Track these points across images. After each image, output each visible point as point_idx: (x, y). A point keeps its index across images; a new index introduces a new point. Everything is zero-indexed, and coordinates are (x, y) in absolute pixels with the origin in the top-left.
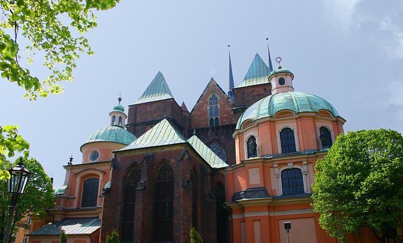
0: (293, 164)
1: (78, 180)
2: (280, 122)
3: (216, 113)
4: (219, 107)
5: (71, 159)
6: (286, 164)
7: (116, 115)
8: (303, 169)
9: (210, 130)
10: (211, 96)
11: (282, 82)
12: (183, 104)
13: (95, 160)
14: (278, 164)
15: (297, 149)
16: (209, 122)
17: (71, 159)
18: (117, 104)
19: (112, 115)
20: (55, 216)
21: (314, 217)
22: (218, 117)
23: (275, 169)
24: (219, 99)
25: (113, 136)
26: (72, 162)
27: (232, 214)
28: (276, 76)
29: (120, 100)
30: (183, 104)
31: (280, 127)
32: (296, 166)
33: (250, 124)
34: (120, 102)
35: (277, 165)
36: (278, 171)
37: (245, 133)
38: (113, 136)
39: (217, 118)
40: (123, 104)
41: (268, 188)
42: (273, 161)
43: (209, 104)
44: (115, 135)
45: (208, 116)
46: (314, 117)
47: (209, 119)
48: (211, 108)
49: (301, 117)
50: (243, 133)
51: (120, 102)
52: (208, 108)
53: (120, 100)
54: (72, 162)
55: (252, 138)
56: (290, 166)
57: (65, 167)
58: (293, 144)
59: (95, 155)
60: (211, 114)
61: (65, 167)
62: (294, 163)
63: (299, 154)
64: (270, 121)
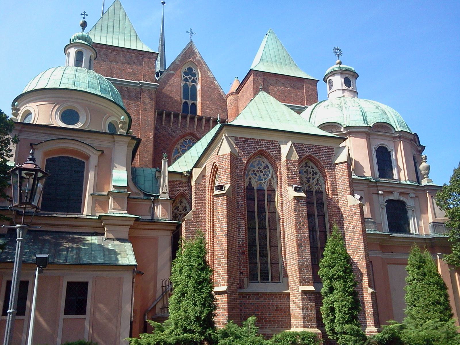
2: (376, 137)
11: (347, 82)
14: (384, 192)
29: (84, 25)
36: (383, 201)
62: (401, 194)
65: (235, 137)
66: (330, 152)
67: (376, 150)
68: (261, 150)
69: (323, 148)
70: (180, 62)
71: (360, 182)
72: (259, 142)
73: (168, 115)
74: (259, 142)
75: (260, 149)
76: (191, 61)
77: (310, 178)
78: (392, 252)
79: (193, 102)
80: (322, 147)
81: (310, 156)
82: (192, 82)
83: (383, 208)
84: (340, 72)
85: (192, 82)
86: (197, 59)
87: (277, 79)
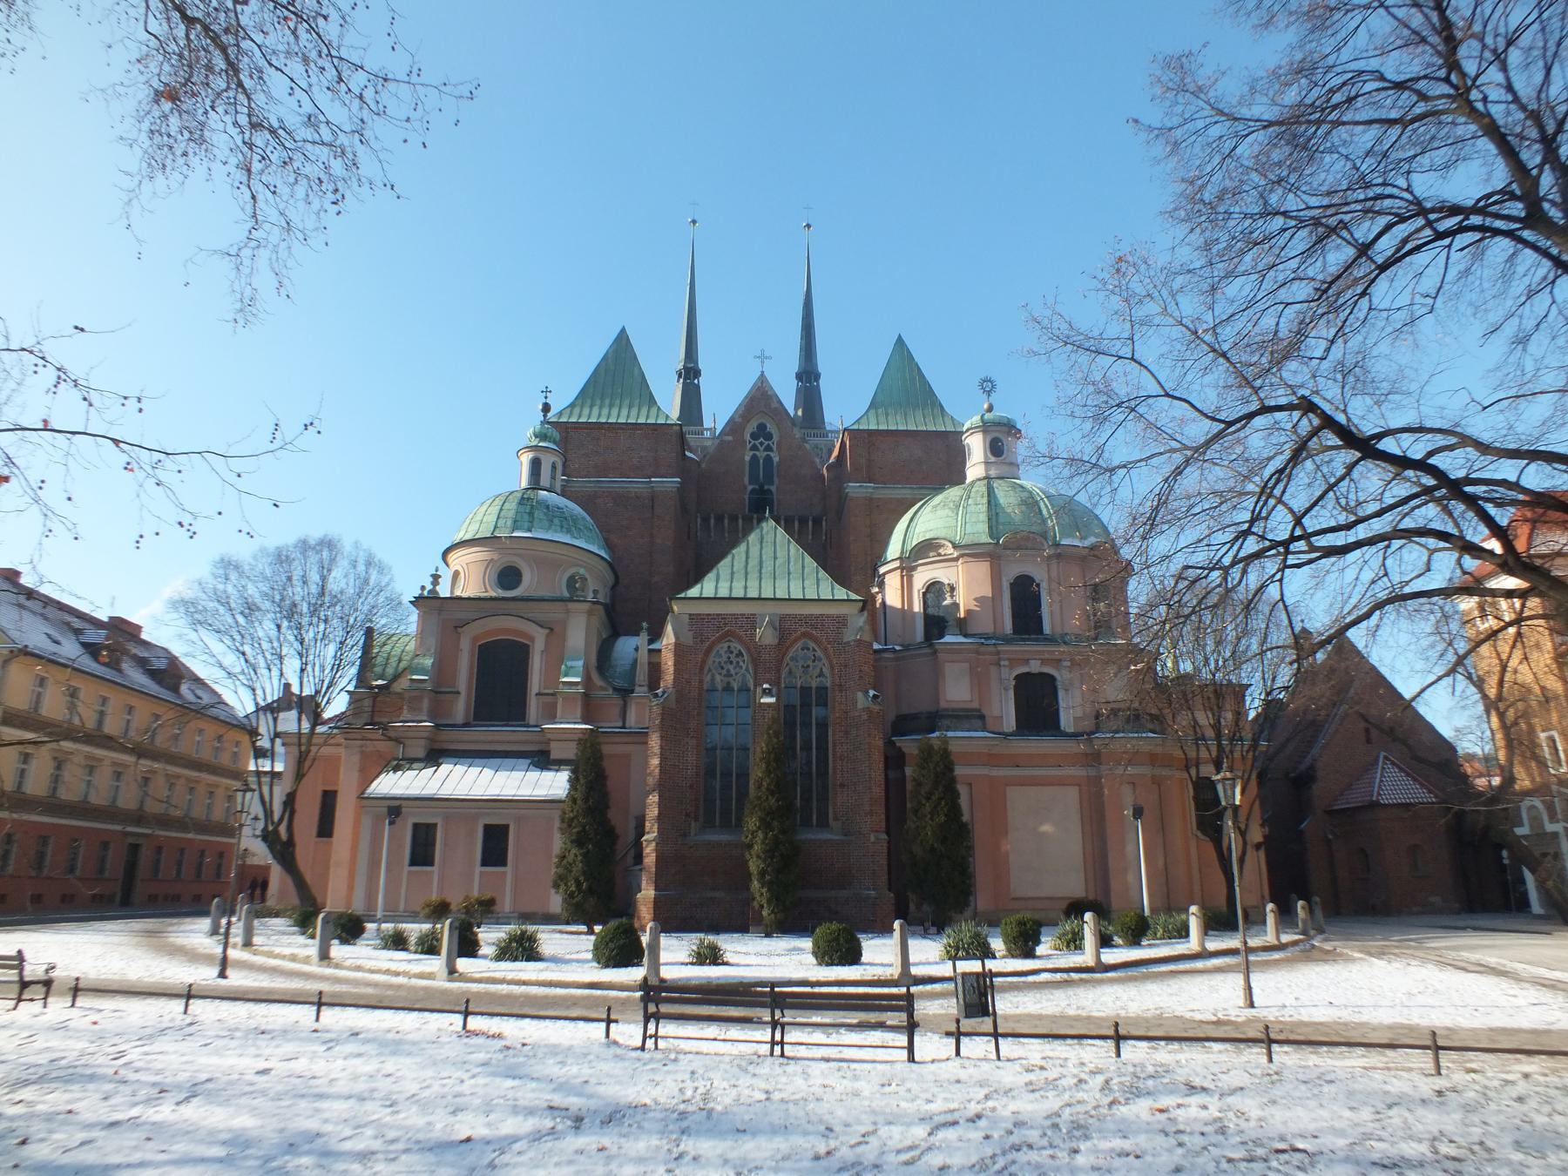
4: (776, 459)
6: (1027, 661)
8: (1062, 676)
15: (1047, 629)
20: (408, 742)
24: (775, 438)
32: (1047, 670)
36: (1010, 675)
43: (749, 446)
45: (746, 480)
46: (1083, 559)
48: (754, 458)
52: (747, 458)
56: (1035, 667)
59: (508, 576)
63: (1051, 640)
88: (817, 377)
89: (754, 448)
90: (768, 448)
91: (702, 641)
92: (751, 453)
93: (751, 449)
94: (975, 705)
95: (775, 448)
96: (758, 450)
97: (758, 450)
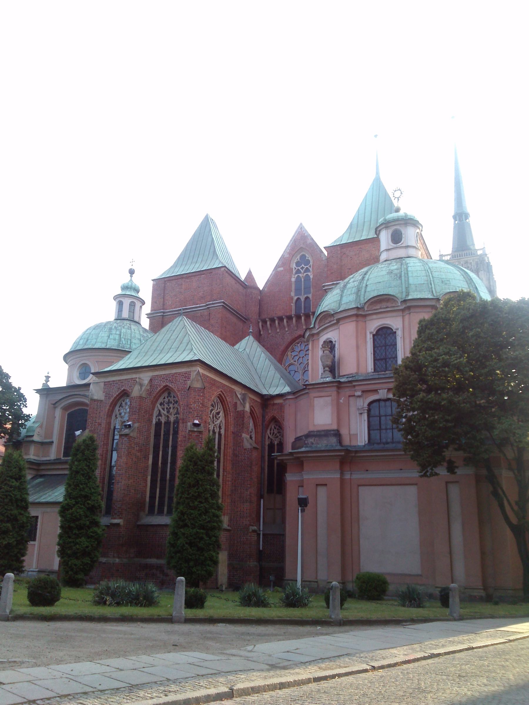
0: (388, 391)
1: (58, 413)
2: (374, 317)
3: (307, 289)
4: (311, 277)
5: (48, 377)
6: (376, 391)
7: (123, 300)
9: (294, 319)
10: (298, 257)
12: (250, 274)
13: (84, 379)
14: (363, 392)
16: (293, 305)
17: (48, 377)
18: (126, 279)
19: (118, 300)
21: (416, 484)
22: (310, 296)
23: (358, 399)
24: (311, 263)
25: (115, 339)
26: (48, 383)
27: (286, 473)
28: (387, 228)
29: (132, 272)
30: (250, 274)
31: (374, 325)
33: (329, 319)
34: (131, 276)
35: (359, 393)
37: (321, 334)
38: (115, 339)
39: (307, 298)
40: (137, 280)
41: (344, 432)
42: (354, 386)
43: (294, 271)
44: (117, 337)
45: (293, 294)
47: (294, 301)
49: (409, 308)
50: (318, 334)
51: (131, 276)
52: (293, 280)
53: (132, 272)
54: (48, 383)
55: (330, 345)
57: (38, 391)
58: (394, 356)
60: (298, 291)
61: (38, 391)
64: (357, 316)
65: (105, 382)
66: (187, 377)
67: (374, 335)
68: (124, 390)
69: (180, 374)
70: (289, 254)
71: (326, 385)
72: (123, 382)
73: (272, 320)
74: (123, 382)
75: (123, 389)
76: (301, 247)
77: (170, 408)
78: (367, 471)
79: (306, 296)
80: (179, 374)
81: (167, 386)
82: (305, 272)
83: (361, 414)
84: (384, 226)
85: (305, 272)
86: (308, 243)
87: (360, 247)
88: (467, 216)
89: (298, 272)
90: (307, 270)
91: (109, 398)
92: (296, 275)
93: (296, 273)
94: (335, 427)
95: (311, 269)
96: (301, 273)
97: (301, 273)
